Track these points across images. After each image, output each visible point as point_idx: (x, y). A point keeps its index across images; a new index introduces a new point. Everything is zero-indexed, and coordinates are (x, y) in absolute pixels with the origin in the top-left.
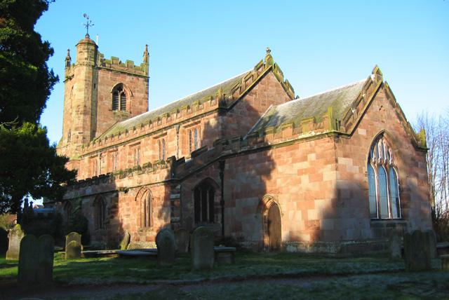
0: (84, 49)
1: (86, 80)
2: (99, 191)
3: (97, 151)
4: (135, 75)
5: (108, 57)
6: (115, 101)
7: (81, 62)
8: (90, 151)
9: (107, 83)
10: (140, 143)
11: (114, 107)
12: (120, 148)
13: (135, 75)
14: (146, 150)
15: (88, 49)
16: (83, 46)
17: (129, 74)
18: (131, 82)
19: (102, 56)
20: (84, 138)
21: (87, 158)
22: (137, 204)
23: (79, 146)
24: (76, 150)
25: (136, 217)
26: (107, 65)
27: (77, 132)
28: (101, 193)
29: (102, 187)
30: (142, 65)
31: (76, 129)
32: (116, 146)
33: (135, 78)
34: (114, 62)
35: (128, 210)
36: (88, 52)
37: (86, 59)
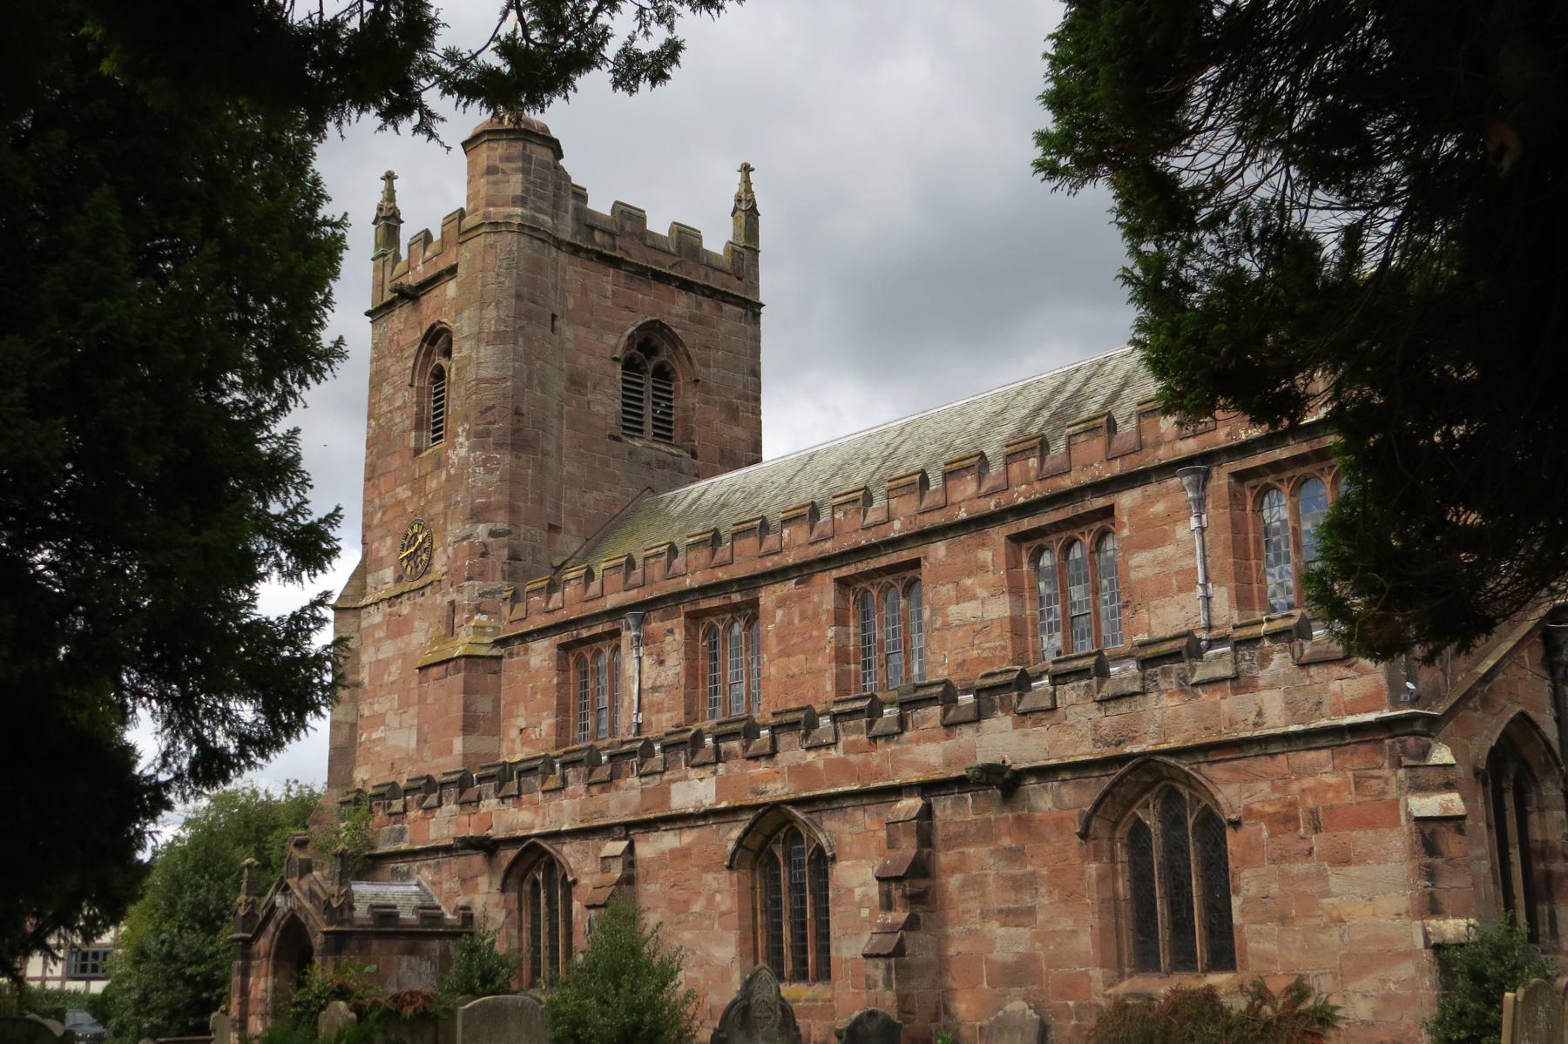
0: (508, 159)
1: (518, 296)
2: (778, 790)
3: (616, 613)
4: (712, 293)
5: (600, 204)
6: (631, 399)
7: (498, 213)
8: (559, 617)
9: (601, 321)
10: (916, 564)
11: (631, 423)
12: (768, 597)
13: (712, 293)
14: (964, 596)
15: (526, 158)
16: (500, 148)
17: (687, 286)
18: (693, 319)
19: (580, 195)
20: (514, 557)
21: (541, 654)
22: (1097, 858)
23: (493, 593)
24: (479, 609)
25: (1093, 920)
26: (597, 236)
27: (482, 530)
28: (798, 803)
29: (799, 771)
30: (732, 248)
31: (477, 515)
32: (753, 582)
33: (707, 305)
34: (628, 228)
35: (1018, 884)
36: (525, 171)
37: (521, 201)
